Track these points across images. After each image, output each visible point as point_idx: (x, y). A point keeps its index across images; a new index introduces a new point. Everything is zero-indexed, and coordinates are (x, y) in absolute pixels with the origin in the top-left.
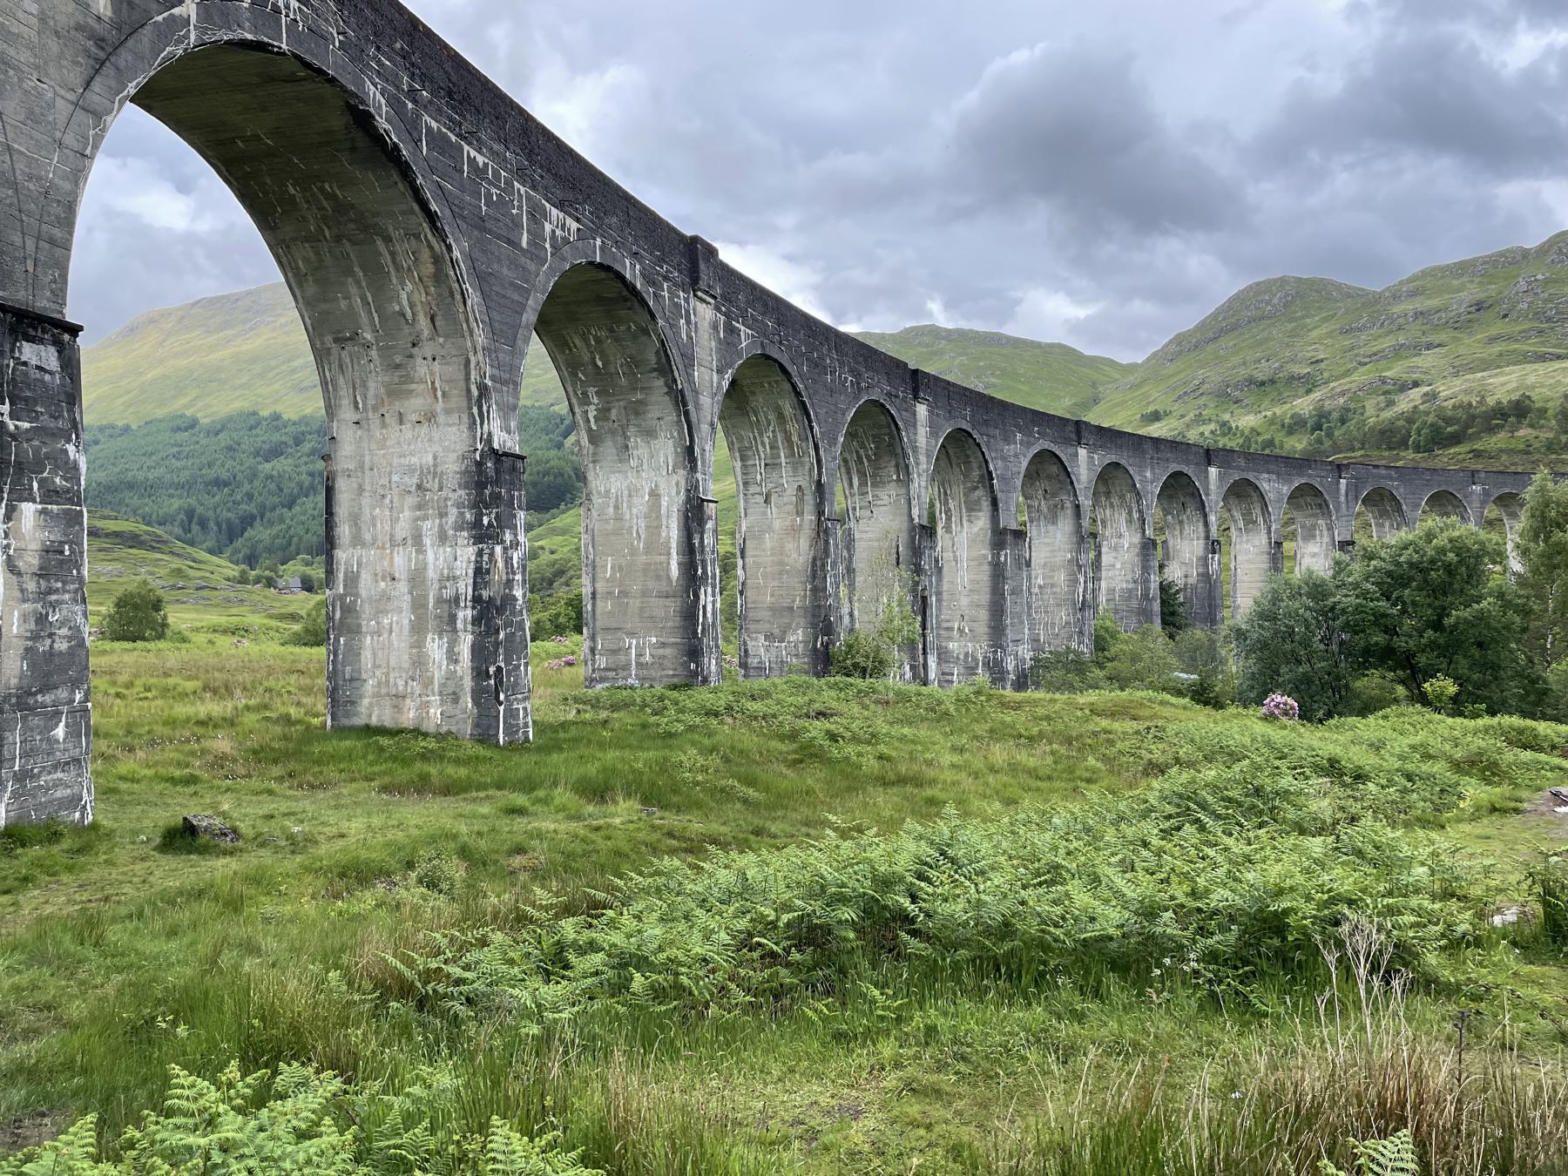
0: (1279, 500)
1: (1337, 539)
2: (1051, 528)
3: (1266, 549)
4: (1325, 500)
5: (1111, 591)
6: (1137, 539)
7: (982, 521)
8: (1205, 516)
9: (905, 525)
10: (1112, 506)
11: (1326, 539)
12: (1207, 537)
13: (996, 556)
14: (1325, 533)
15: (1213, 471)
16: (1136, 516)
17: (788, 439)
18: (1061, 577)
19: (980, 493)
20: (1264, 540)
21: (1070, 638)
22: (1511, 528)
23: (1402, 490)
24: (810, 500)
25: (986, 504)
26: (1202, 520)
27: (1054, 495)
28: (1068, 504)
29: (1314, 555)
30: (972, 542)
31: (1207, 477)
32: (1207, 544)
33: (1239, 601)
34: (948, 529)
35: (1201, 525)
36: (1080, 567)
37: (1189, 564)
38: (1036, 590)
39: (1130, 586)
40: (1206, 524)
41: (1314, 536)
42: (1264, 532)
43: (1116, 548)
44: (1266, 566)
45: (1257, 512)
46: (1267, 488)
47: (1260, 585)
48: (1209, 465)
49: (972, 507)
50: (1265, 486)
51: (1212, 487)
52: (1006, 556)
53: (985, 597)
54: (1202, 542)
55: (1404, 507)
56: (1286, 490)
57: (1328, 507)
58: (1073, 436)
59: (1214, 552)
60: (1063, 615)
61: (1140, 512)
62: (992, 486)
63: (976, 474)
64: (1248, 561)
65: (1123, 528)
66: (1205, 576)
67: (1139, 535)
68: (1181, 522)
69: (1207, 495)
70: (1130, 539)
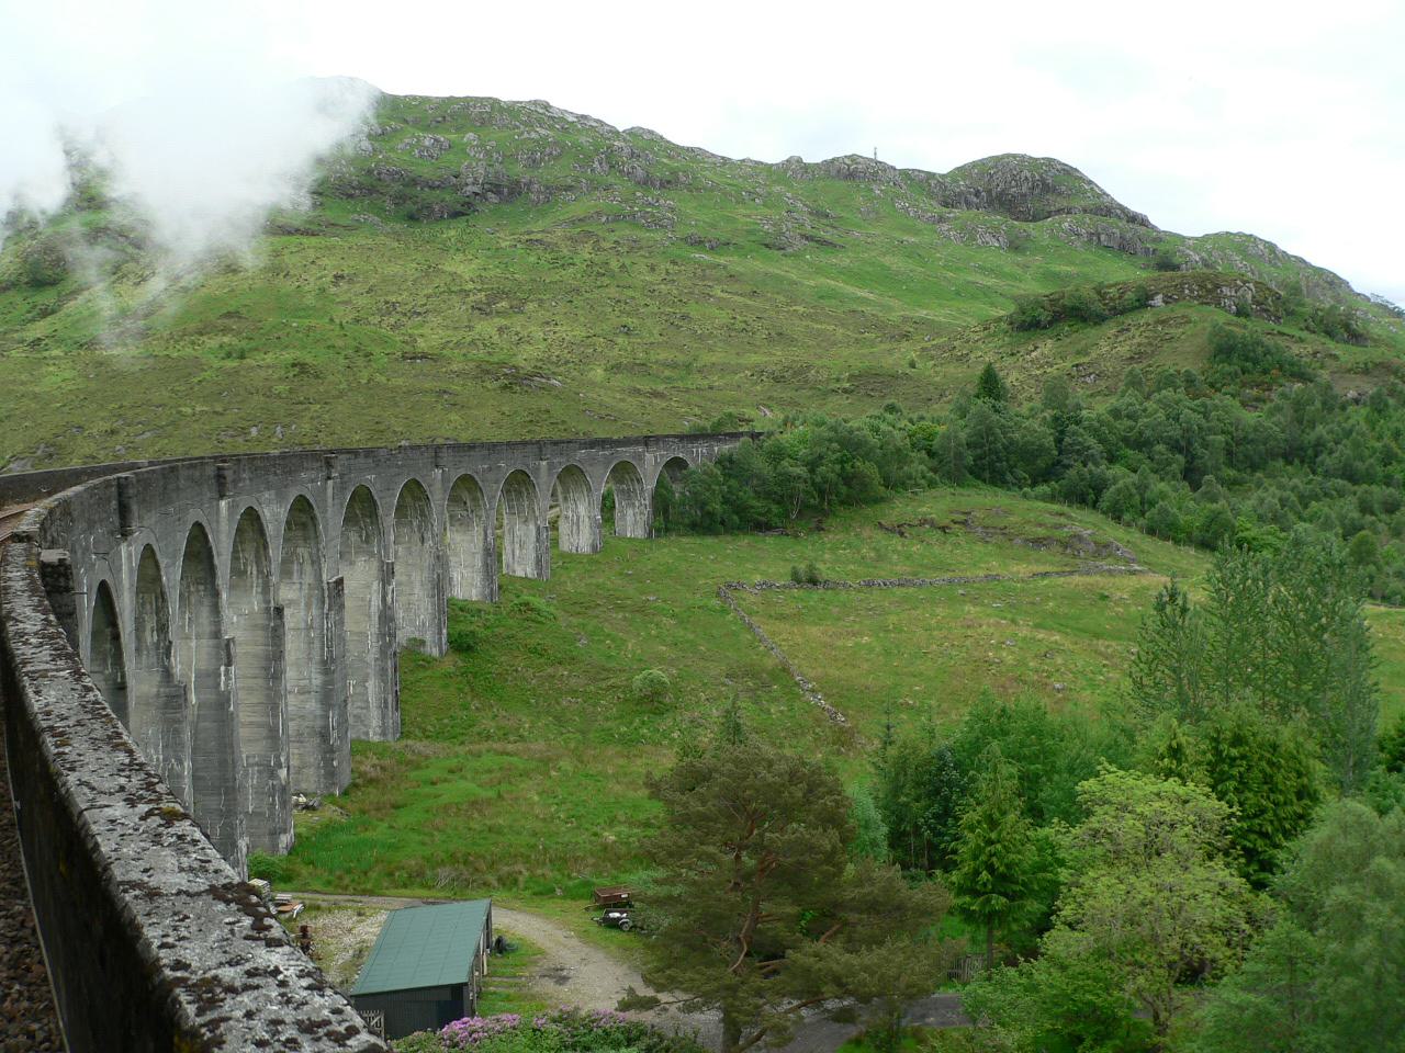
0: (277, 536)
1: (324, 577)
3: (261, 621)
4: (313, 518)
8: (216, 594)
11: (309, 579)
14: (308, 568)
15: (223, 503)
22: (451, 517)
23: (378, 486)
26: (206, 602)
31: (218, 522)
32: (217, 647)
40: (216, 609)
44: (260, 649)
45: (249, 555)
47: (251, 682)
48: (222, 496)
50: (266, 513)
51: (223, 537)
54: (206, 643)
55: (380, 512)
56: (283, 512)
57: (315, 526)
58: (115, 519)
59: (229, 664)
67: (157, 678)
69: (218, 555)
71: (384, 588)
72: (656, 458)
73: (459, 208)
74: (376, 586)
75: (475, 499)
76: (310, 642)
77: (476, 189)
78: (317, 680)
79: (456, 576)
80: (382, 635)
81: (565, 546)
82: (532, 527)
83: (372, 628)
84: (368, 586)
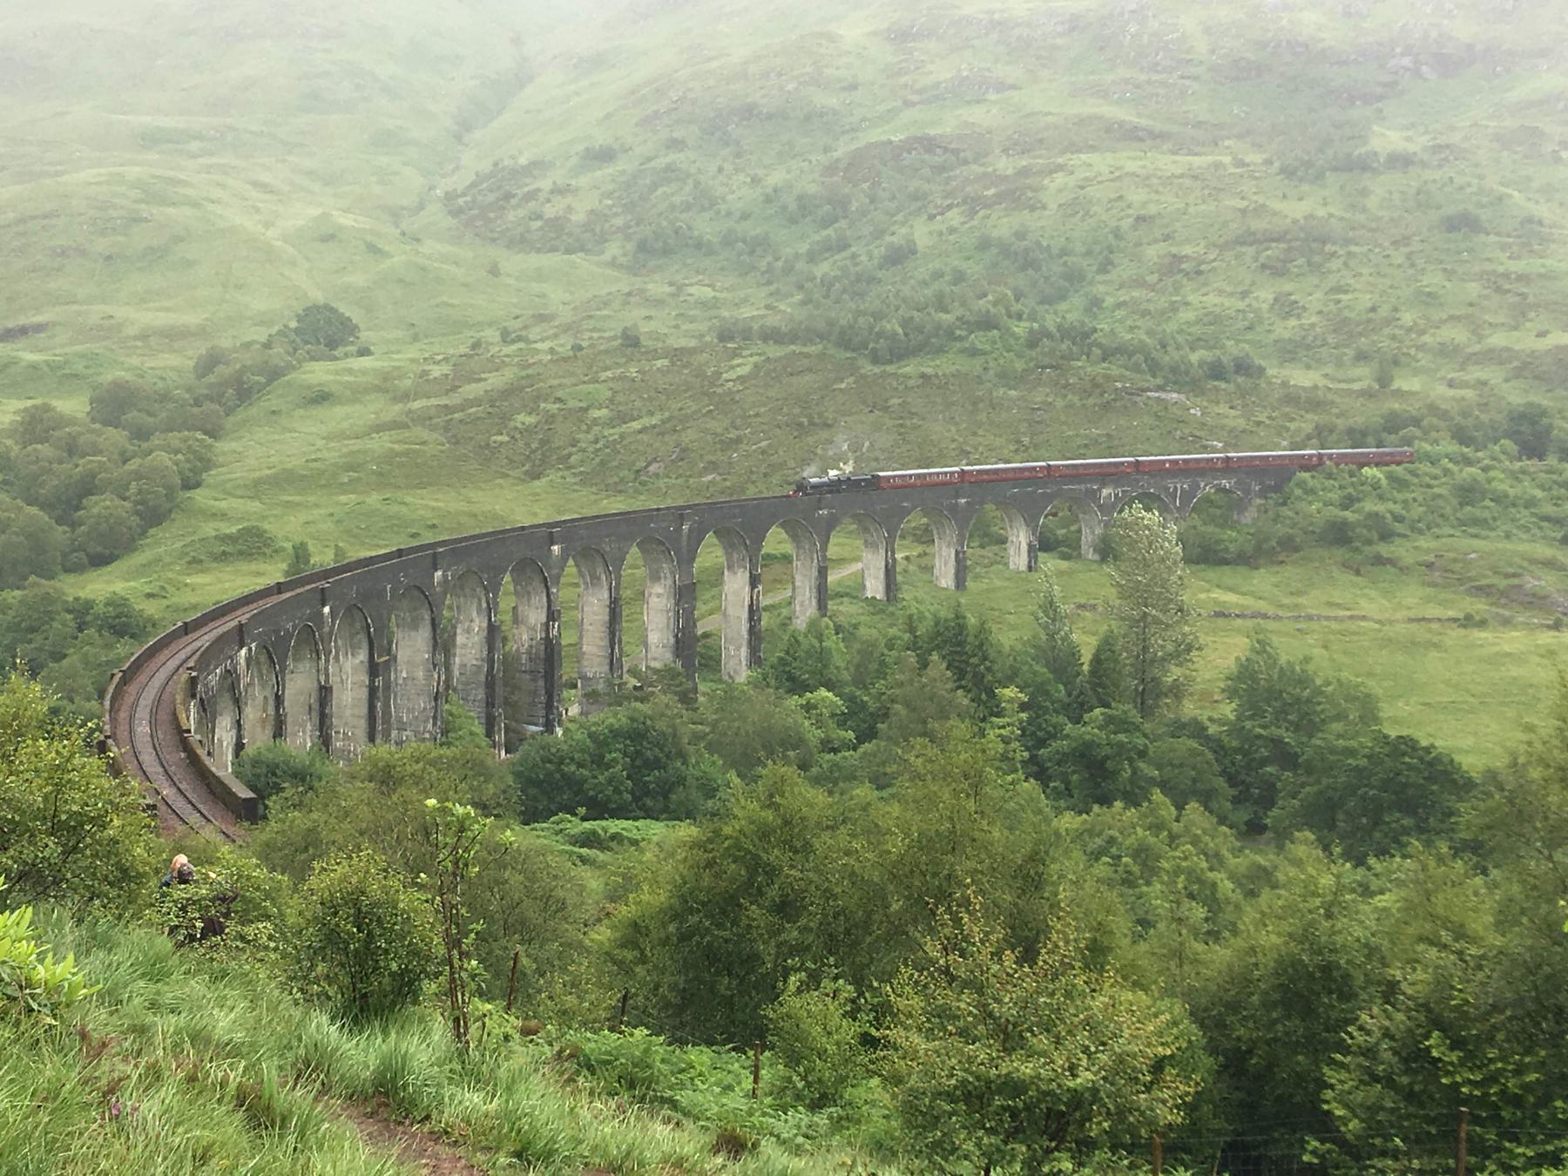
2: (413, 634)
5: (463, 666)
6: (485, 625)
7: (363, 656)
8: (548, 589)
9: (316, 684)
10: (465, 596)
11: (669, 582)
12: (549, 607)
13: (372, 681)
15: (555, 548)
16: (484, 605)
17: (260, 672)
18: (420, 674)
19: (362, 637)
20: (606, 595)
21: (426, 721)
24: (271, 703)
25: (365, 645)
27: (415, 609)
28: (427, 617)
29: (659, 596)
30: (355, 669)
33: (585, 648)
34: (337, 658)
35: (545, 599)
36: (435, 666)
37: (533, 629)
38: (400, 682)
39: (480, 663)
41: (660, 578)
42: (606, 587)
43: (468, 631)
45: (600, 570)
46: (608, 549)
49: (354, 648)
52: (379, 681)
53: (364, 710)
59: (554, 621)
60: (423, 703)
61: (488, 604)
62: (369, 632)
63: (358, 625)
64: (595, 614)
65: (474, 614)
66: (548, 641)
68: (529, 593)
70: (479, 624)
71: (752, 590)
72: (1116, 495)
73: (1379, 90)
74: (747, 589)
75: (876, 530)
76: (669, 618)
77: (1406, 61)
78: (672, 640)
79: (868, 584)
80: (751, 619)
81: (1012, 566)
82: (953, 552)
83: (745, 615)
84: (743, 588)
